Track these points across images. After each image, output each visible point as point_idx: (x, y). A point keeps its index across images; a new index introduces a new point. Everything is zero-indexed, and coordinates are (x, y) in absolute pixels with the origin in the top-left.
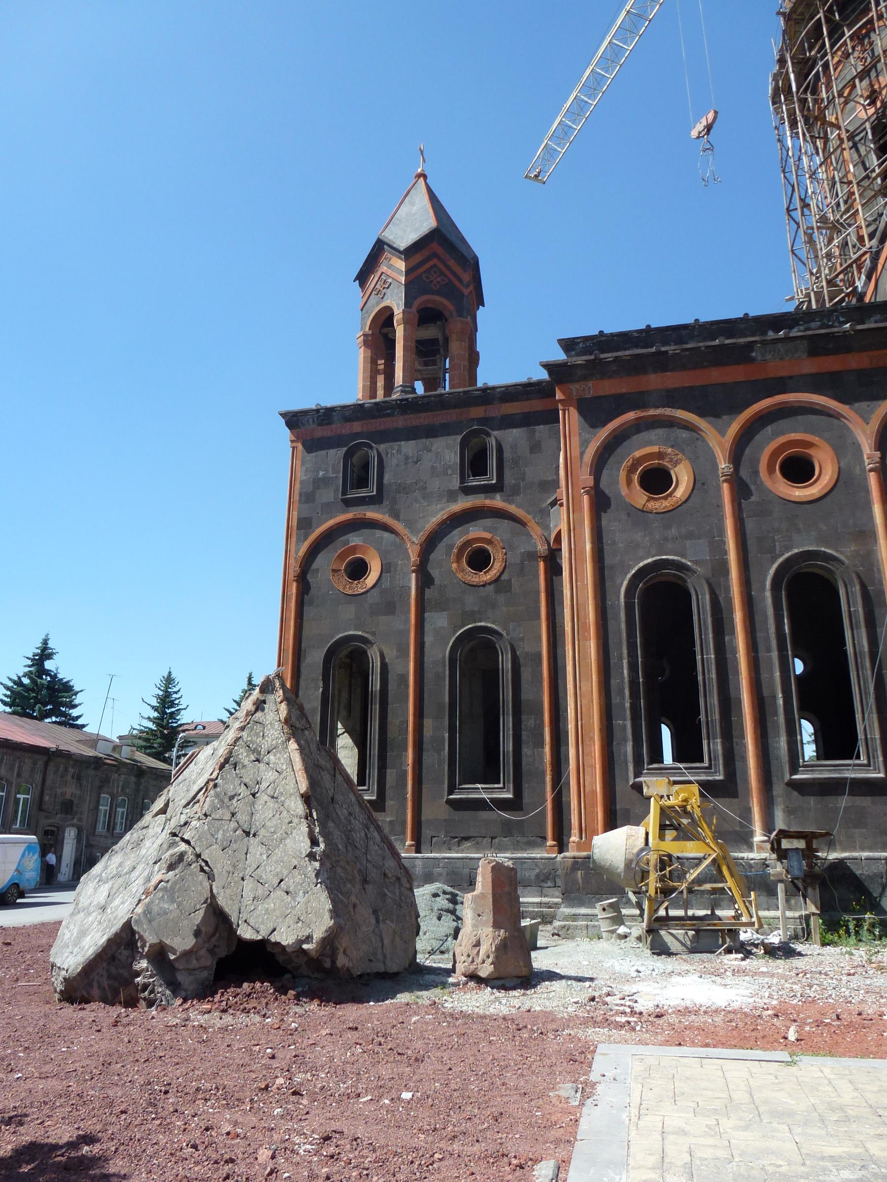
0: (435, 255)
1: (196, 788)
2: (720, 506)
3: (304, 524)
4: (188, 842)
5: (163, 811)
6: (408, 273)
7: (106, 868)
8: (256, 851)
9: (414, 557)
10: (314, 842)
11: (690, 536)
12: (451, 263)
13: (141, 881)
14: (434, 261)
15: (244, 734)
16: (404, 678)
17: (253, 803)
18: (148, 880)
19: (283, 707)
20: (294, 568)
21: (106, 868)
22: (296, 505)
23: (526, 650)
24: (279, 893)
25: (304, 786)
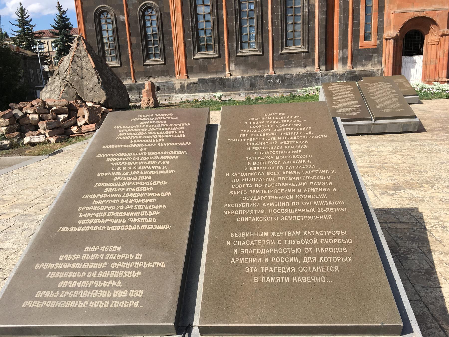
1: (66, 68)
4: (68, 81)
5: (58, 74)
7: (46, 89)
8: (85, 83)
10: (99, 80)
13: (58, 91)
15: (76, 53)
16: (124, 22)
17: (82, 71)
18: (60, 90)
19: (84, 45)
21: (46, 89)
23: (165, 11)
24: (92, 91)
25: (94, 66)
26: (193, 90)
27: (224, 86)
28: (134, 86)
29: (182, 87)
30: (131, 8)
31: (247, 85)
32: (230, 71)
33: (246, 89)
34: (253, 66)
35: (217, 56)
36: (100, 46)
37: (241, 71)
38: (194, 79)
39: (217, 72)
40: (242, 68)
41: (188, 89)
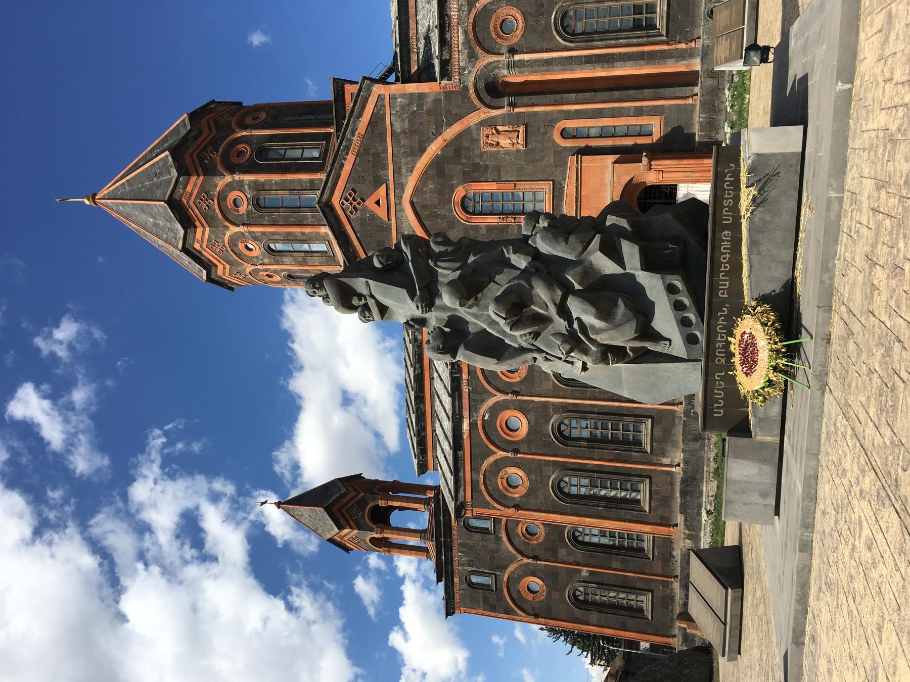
0: (340, 510)
2: (529, 459)
3: (508, 611)
6: (351, 528)
9: (530, 561)
11: (541, 473)
12: (345, 500)
14: (344, 510)
16: (590, 572)
20: (531, 619)
22: (497, 614)
26: (695, 523)
27: (695, 479)
28: (683, 582)
29: (689, 537)
30: (572, 559)
31: (696, 446)
32: (671, 466)
33: (702, 447)
34: (668, 432)
35: (648, 480)
36: (621, 612)
37: (674, 450)
38: (680, 519)
39: (672, 484)
40: (669, 448)
41: (693, 531)
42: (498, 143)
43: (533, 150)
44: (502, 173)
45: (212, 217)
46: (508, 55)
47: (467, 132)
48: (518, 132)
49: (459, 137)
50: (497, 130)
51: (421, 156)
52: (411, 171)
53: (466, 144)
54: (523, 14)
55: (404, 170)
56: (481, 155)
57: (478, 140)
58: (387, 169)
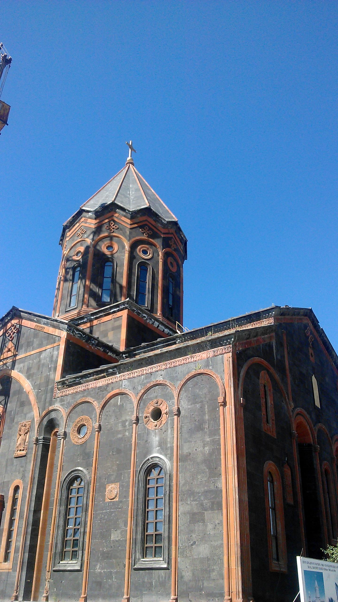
42: (20, 435)
43: (12, 464)
44: (5, 441)
45: (73, 240)
46: (62, 434)
47: (31, 410)
48: (23, 450)
49: (30, 403)
50: (27, 433)
51: (25, 376)
52: (20, 371)
53: (26, 409)
54: (85, 442)
55: (22, 365)
56: (17, 423)
57: (25, 419)
58: (24, 353)
